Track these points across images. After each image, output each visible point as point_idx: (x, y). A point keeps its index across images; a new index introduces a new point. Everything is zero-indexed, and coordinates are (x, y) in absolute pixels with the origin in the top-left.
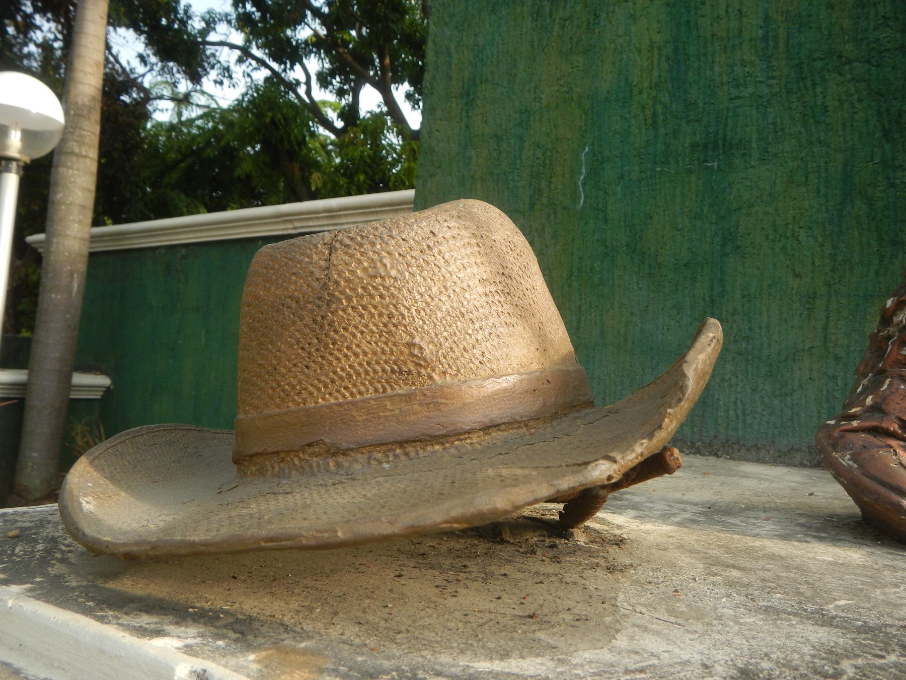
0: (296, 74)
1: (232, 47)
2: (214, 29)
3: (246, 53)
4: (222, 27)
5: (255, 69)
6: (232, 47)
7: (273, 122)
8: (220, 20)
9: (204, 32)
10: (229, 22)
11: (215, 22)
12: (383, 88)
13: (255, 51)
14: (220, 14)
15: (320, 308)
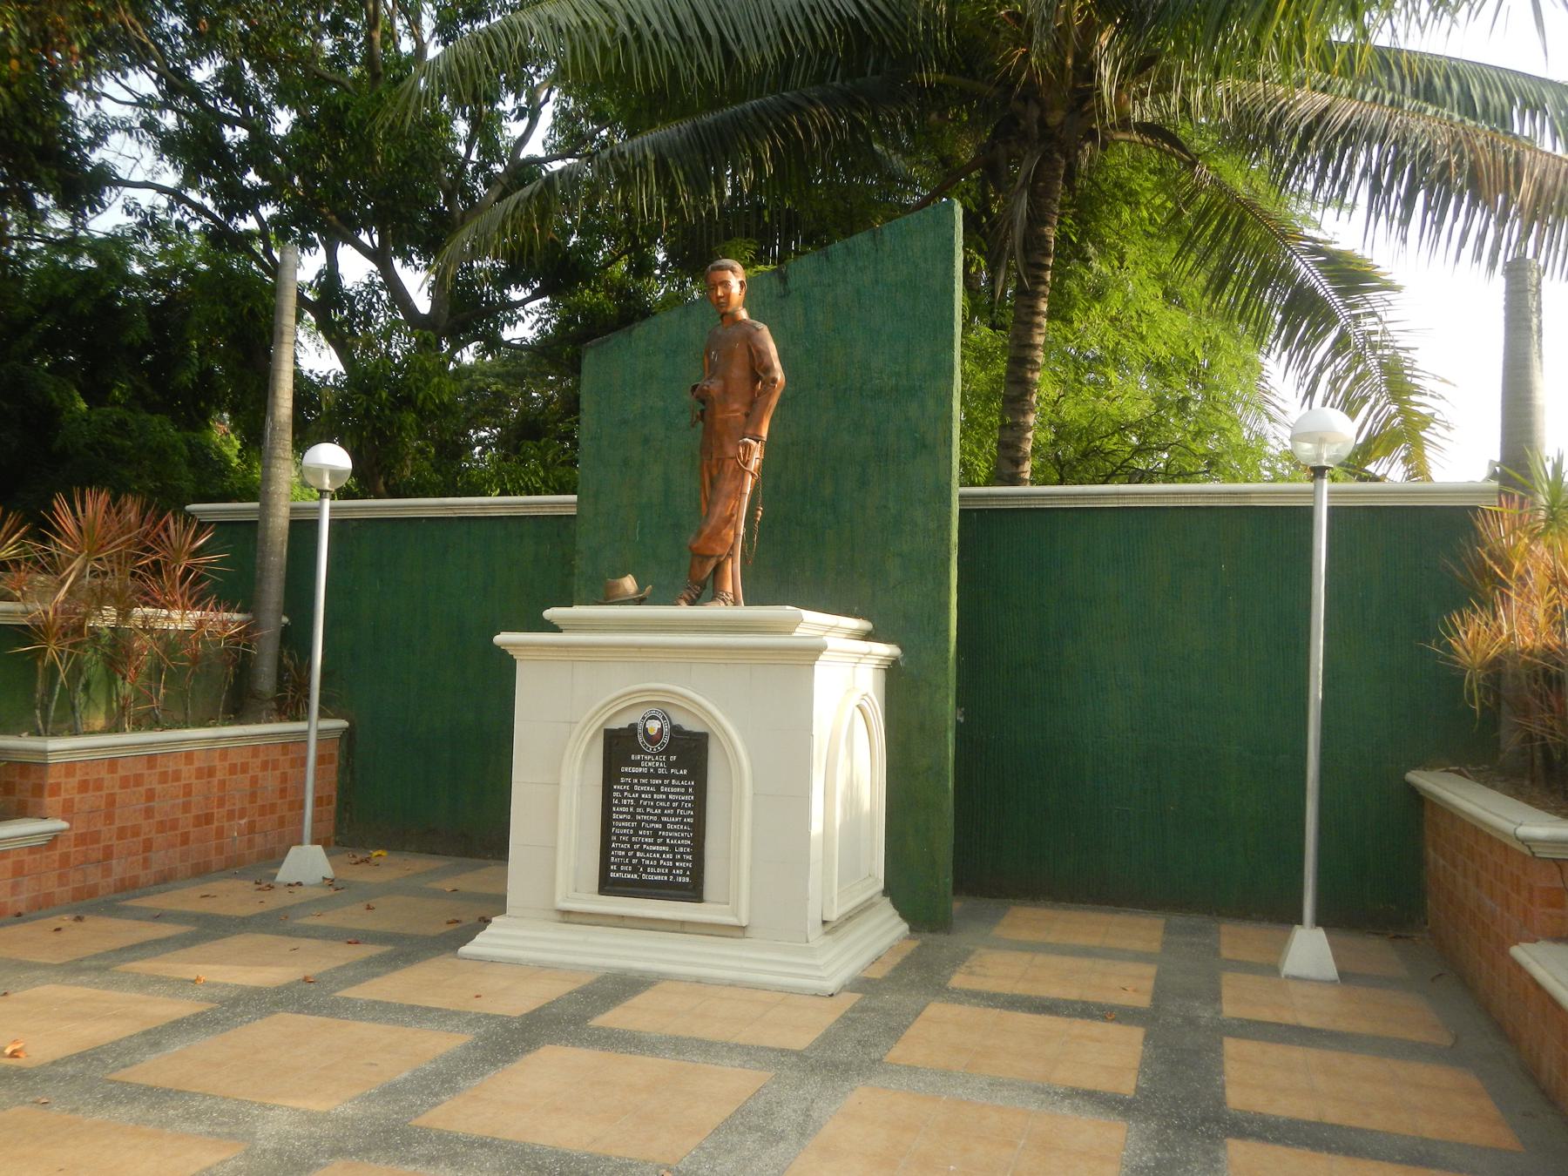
0: (251, 224)
1: (161, 190)
2: (105, 139)
3: (177, 196)
4: (116, 139)
5: (193, 219)
6: (161, 190)
7: (251, 311)
8: (115, 128)
9: (93, 144)
10: (129, 131)
11: (104, 130)
12: (379, 256)
13: (194, 196)
14: (114, 119)
15: (618, 586)
